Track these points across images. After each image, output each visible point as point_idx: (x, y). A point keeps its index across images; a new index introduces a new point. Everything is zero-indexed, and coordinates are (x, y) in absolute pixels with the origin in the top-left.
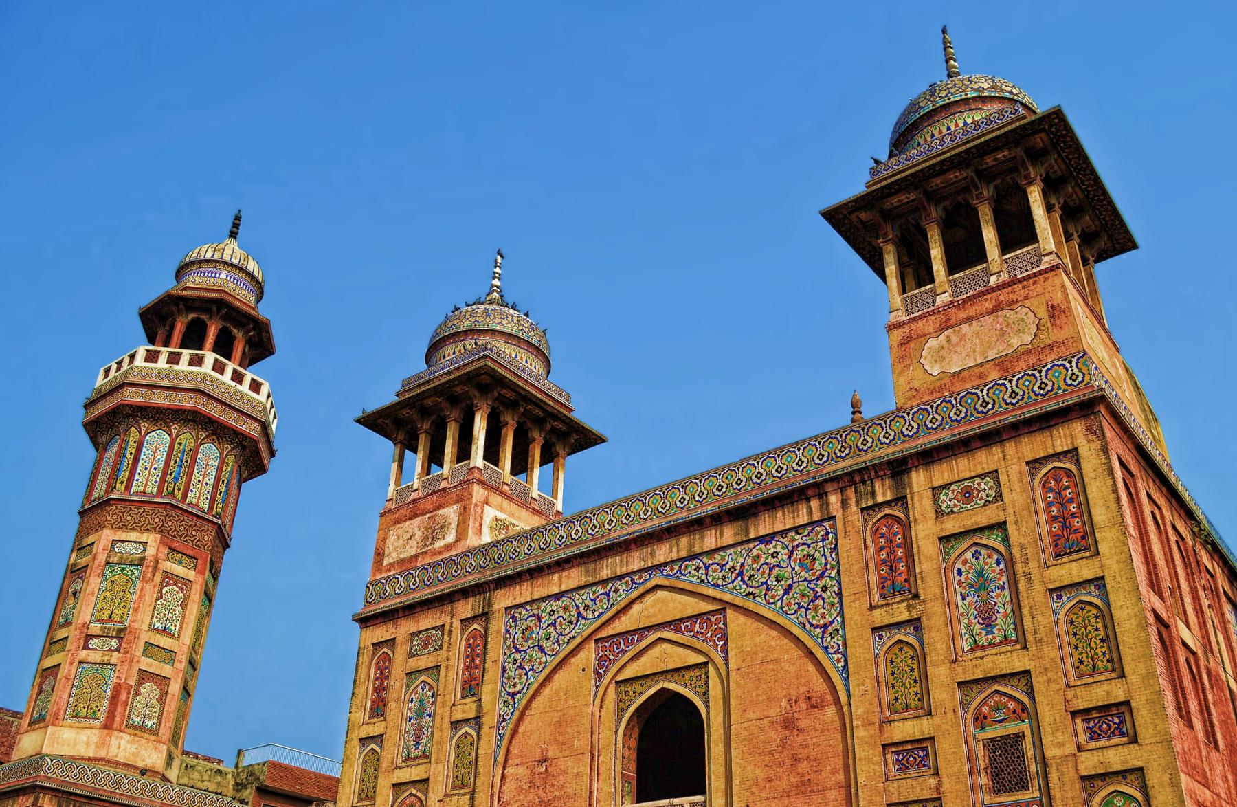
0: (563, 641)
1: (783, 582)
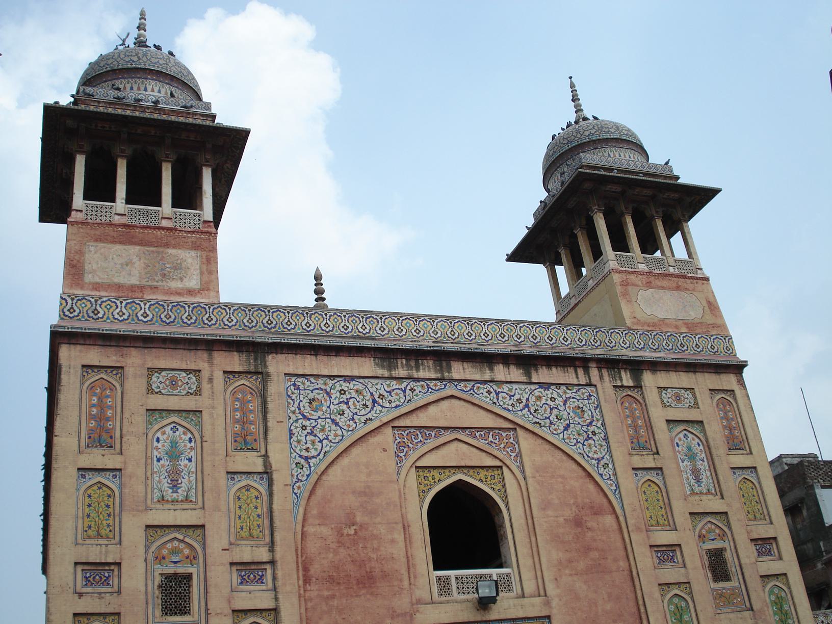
0: (359, 420)
1: (562, 421)
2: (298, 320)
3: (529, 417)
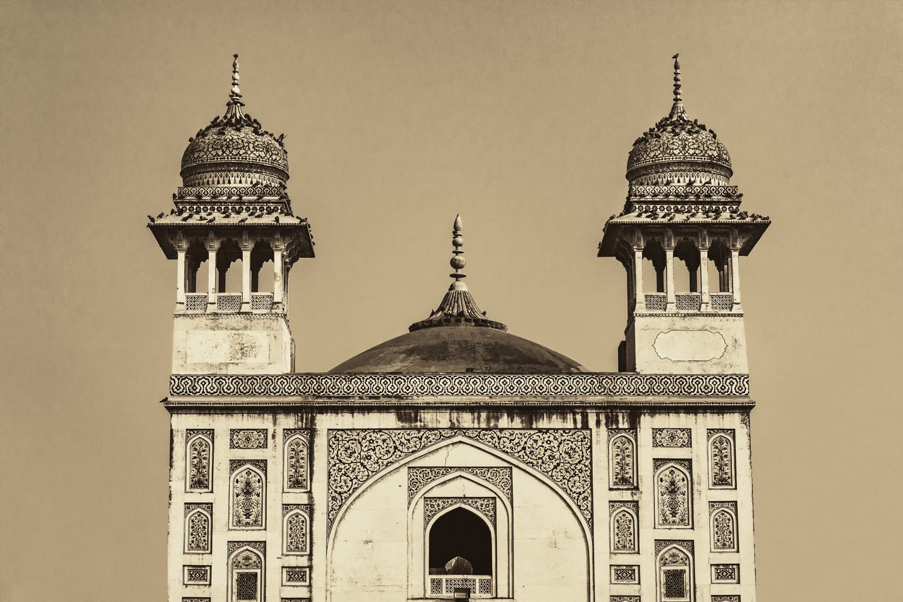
0: (382, 463)
1: (553, 461)
2: (341, 385)
3: (524, 458)
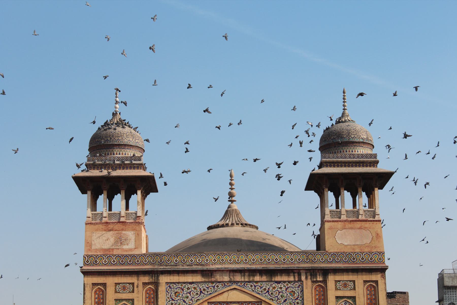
0: (194, 300)
1: (283, 298)
2: (172, 259)
3: (268, 297)
